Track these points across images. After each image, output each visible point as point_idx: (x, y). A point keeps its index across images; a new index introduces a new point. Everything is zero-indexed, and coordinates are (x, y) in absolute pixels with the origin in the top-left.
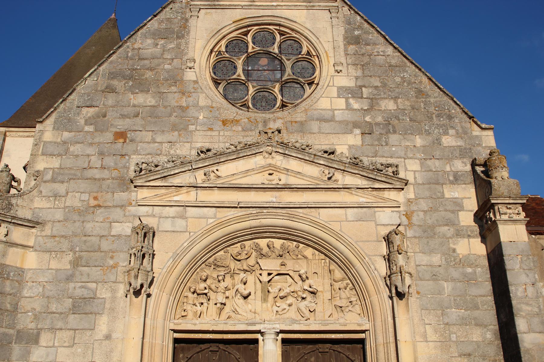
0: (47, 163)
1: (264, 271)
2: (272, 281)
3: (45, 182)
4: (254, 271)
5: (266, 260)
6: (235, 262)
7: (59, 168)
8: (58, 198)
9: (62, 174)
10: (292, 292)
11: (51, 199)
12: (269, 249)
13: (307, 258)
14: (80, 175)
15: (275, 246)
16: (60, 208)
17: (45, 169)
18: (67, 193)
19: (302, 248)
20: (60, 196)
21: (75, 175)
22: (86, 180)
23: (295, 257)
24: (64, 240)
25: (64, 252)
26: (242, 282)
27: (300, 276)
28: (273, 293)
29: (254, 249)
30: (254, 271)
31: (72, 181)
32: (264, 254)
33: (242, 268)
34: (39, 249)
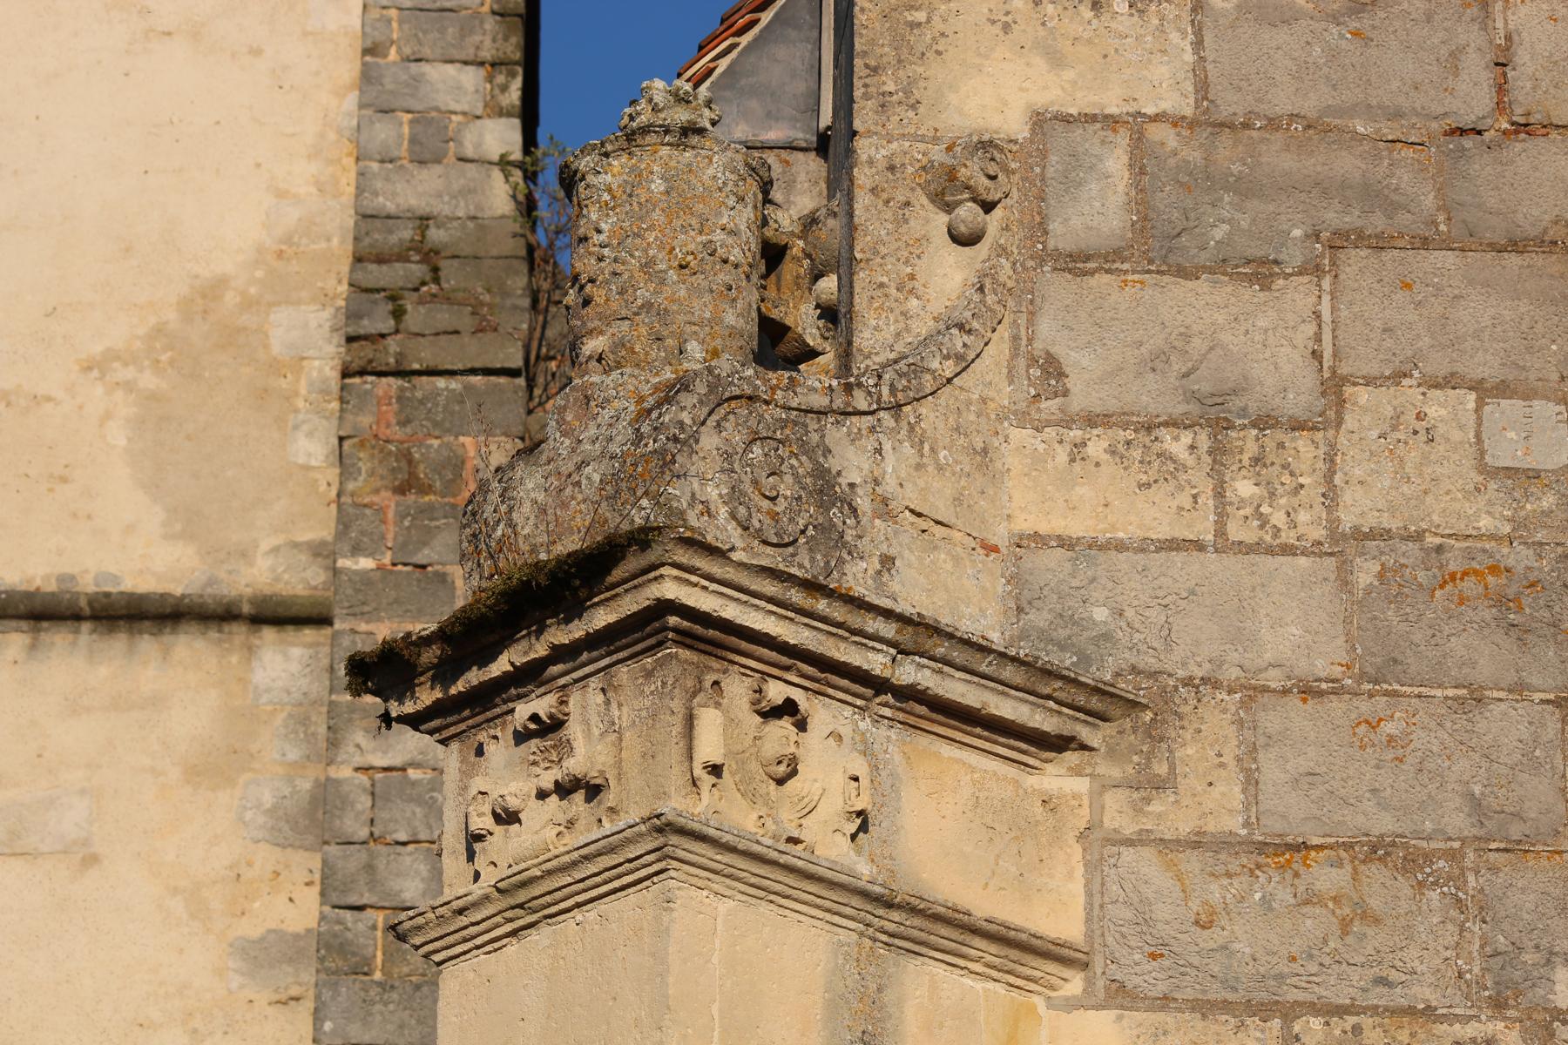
0: (1057, 61)
3: (1076, 263)
7: (1193, 124)
8: (1248, 442)
9: (1245, 189)
11: (1177, 445)
14: (1429, 201)
16: (1288, 550)
17: (1041, 121)
18: (1334, 387)
20: (1264, 422)
21: (1373, 195)
22: (1513, 260)
24: (1404, 886)
25: (1429, 1013)
31: (1355, 261)
34: (1149, 978)
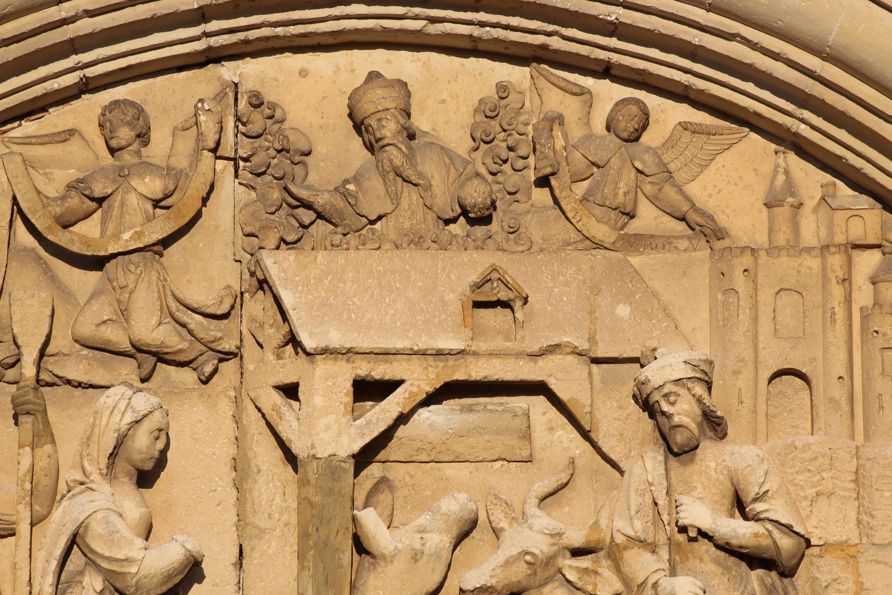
1: (323, 366)
2: (392, 451)
4: (226, 356)
5: (340, 258)
6: (53, 279)
10: (577, 553)
12: (370, 148)
13: (719, 234)
15: (421, 121)
19: (670, 143)
23: (602, 232)
26: (121, 465)
27: (647, 405)
28: (398, 566)
29: (227, 149)
30: (226, 356)
32: (321, 200)
33: (117, 336)
